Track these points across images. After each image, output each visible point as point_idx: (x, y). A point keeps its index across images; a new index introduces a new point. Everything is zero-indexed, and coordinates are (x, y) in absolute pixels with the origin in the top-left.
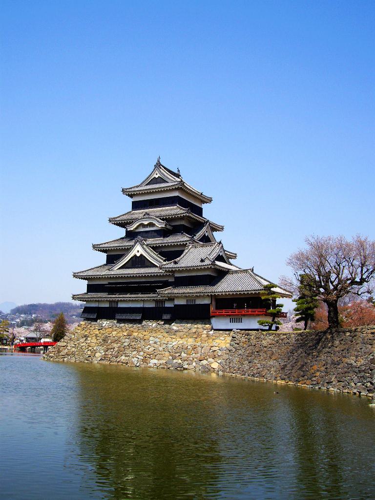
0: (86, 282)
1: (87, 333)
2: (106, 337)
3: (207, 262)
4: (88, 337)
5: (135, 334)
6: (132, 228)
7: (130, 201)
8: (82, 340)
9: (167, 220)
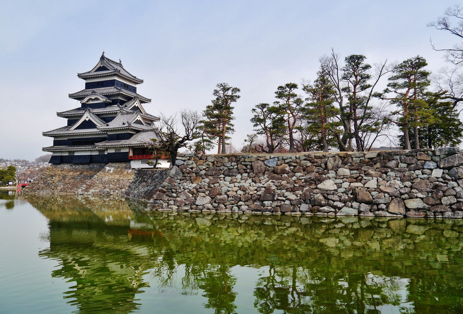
2: (66, 176)
3: (127, 125)
5: (85, 173)
7: (83, 82)
9: (107, 96)
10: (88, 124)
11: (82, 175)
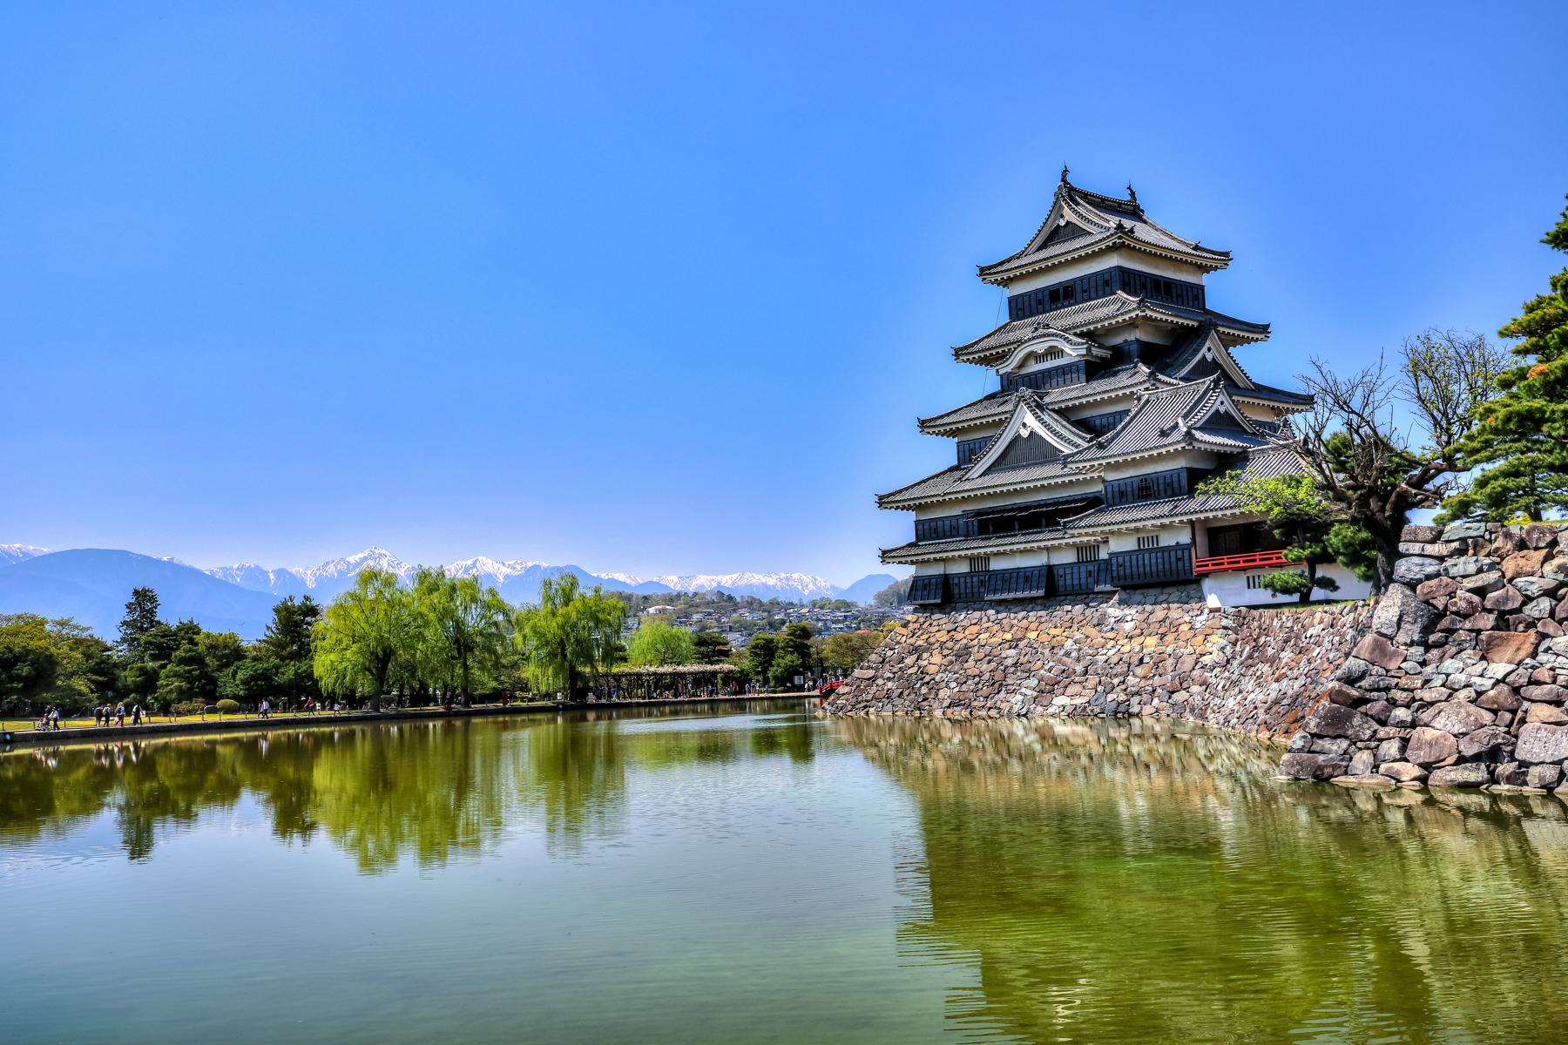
0: (911, 516)
1: (920, 642)
4: (926, 650)
6: (1009, 366)
8: (909, 661)
10: (1029, 451)
11: (1022, 644)
